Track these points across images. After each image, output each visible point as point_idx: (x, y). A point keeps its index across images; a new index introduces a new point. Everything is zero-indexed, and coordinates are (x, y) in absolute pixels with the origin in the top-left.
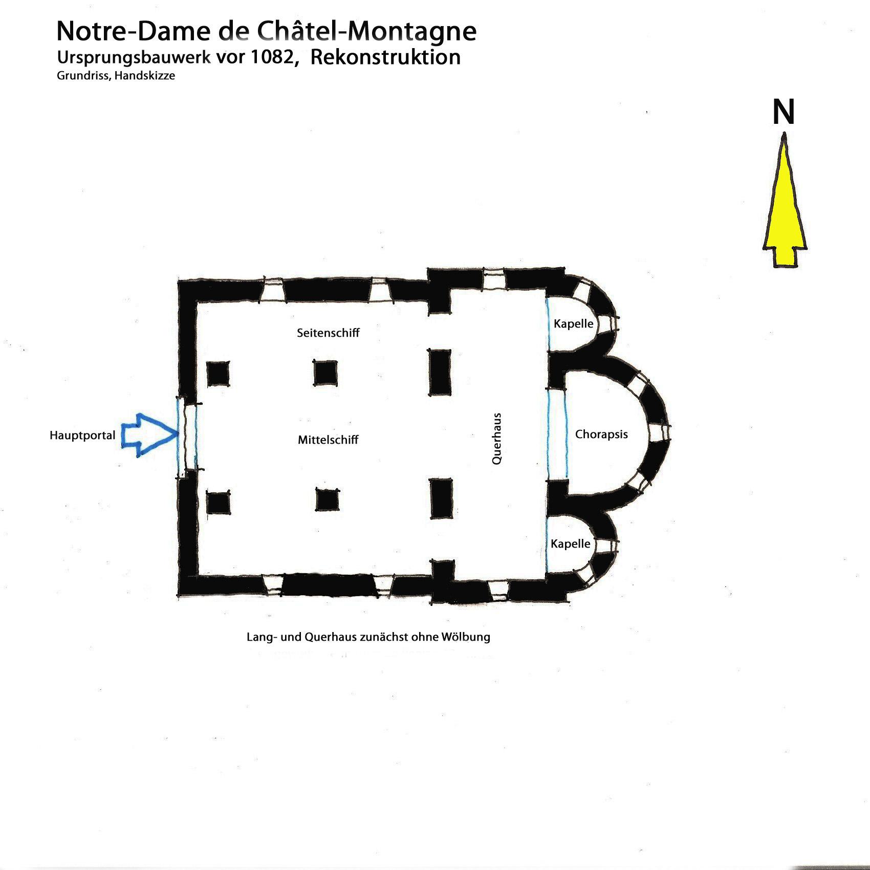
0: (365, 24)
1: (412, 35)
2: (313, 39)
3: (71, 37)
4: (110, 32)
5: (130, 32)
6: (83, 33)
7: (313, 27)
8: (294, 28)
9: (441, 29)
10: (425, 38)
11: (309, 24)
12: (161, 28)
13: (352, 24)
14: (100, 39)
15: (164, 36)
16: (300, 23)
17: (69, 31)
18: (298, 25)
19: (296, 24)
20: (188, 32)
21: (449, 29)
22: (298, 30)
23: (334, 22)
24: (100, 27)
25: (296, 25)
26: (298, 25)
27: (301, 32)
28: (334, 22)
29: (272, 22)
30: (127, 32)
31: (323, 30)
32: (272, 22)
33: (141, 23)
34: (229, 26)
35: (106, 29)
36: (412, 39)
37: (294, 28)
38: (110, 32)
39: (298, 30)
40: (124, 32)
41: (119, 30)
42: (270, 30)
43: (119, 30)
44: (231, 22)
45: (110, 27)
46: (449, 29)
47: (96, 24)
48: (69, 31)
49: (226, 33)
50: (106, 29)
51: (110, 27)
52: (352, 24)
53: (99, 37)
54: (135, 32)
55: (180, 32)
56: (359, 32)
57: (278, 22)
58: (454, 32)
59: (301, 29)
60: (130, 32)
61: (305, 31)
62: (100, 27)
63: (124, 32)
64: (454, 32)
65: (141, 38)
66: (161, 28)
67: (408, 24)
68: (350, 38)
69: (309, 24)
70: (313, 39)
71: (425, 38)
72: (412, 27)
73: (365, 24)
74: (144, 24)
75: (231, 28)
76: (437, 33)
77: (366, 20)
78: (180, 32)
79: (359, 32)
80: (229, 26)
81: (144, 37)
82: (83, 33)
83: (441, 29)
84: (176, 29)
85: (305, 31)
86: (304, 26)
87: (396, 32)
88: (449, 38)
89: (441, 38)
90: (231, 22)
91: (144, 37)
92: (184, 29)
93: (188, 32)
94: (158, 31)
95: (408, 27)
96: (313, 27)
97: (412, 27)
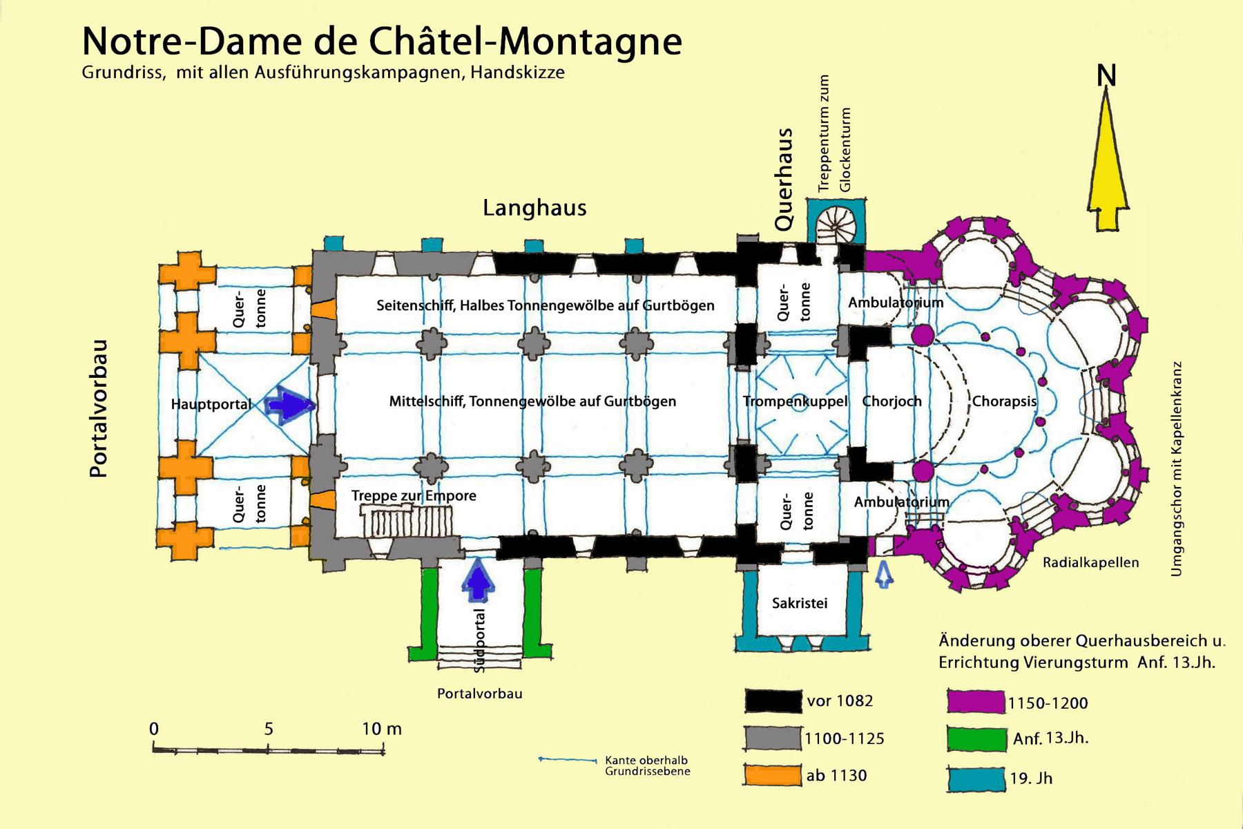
0: (524, 31)
1: (591, 47)
2: (449, 53)
3: (102, 50)
4: (159, 43)
5: (187, 43)
6: (121, 44)
7: (449, 36)
8: (422, 36)
9: (632, 38)
10: (609, 51)
11: (444, 32)
12: (231, 36)
13: (505, 31)
14: (144, 53)
15: (235, 48)
16: (430, 31)
17: (101, 44)
18: (427, 32)
19: (424, 31)
20: (270, 42)
21: (643, 38)
22: (427, 39)
23: (478, 28)
24: (144, 36)
25: (424, 33)
26: (427, 32)
27: (432, 43)
28: (478, 28)
29: (390, 29)
30: (183, 42)
31: (463, 40)
32: (390, 29)
33: (203, 30)
34: (329, 34)
35: (153, 38)
36: (590, 53)
37: (422, 36)
38: (159, 43)
39: (427, 39)
40: (178, 43)
41: (172, 40)
42: (386, 40)
43: (172, 40)
44: (332, 28)
45: (159, 36)
46: (643, 38)
47: (139, 32)
48: (101, 44)
49: (324, 44)
50: (153, 38)
51: (159, 36)
52: (505, 31)
53: (143, 50)
54: (194, 43)
55: (258, 42)
56: (515, 43)
57: (398, 28)
58: (650, 43)
59: (431, 37)
60: (187, 43)
61: (438, 42)
62: (144, 36)
63: (178, 43)
64: (650, 43)
65: (203, 52)
66: (231, 36)
67: (585, 32)
68: (503, 52)
69: (444, 32)
70: (449, 53)
71: (609, 51)
72: (591, 36)
73: (524, 31)
74: (207, 31)
75: (331, 38)
76: (625, 44)
77: (524, 26)
78: (258, 42)
79: (515, 43)
80: (329, 34)
81: (206, 50)
82: (121, 44)
83: (632, 38)
84: (252, 38)
85: (438, 42)
86: (435, 34)
87: (567, 43)
88: (643, 52)
89: (632, 50)
90: (332, 28)
91: (206, 50)
92: (264, 39)
93: (270, 42)
94: (227, 41)
95: (585, 35)
96: (449, 36)
97: (591, 36)
